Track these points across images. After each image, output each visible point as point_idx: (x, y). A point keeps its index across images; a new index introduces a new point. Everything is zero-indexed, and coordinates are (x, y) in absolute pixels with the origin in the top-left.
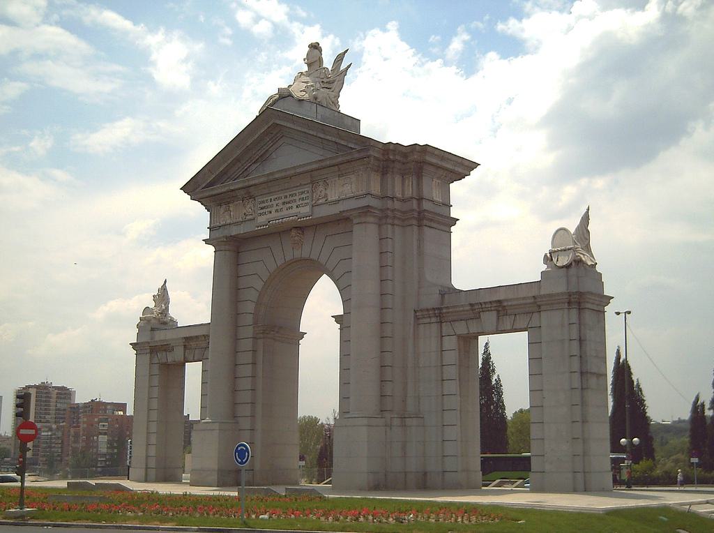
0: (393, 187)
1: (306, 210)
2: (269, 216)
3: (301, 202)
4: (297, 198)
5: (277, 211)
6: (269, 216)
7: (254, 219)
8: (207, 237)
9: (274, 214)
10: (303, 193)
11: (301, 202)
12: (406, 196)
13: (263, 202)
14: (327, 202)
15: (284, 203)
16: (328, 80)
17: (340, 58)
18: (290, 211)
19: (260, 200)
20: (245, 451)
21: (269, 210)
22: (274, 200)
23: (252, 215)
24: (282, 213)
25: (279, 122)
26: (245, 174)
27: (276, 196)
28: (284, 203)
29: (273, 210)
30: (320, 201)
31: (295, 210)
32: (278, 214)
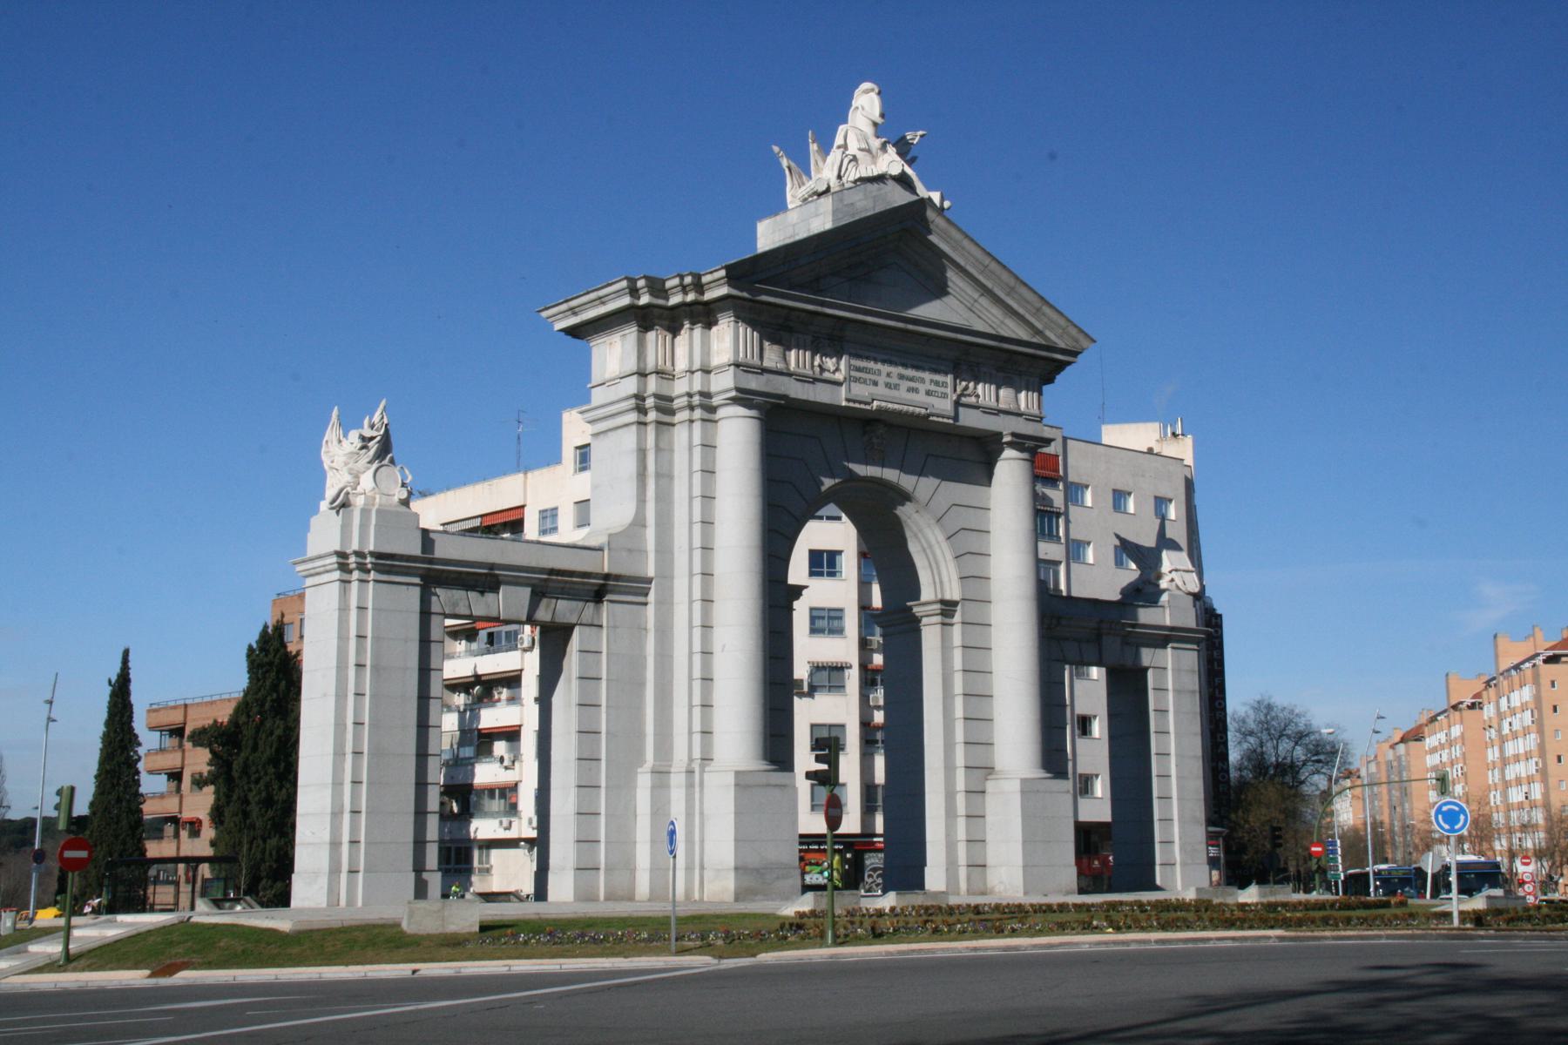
1: (946, 406)
3: (933, 388)
5: (888, 385)
6: (872, 389)
9: (881, 390)
11: (933, 388)
15: (901, 377)
20: (1442, 813)
21: (874, 377)
24: (894, 393)
28: (901, 377)
29: (882, 380)
31: (921, 398)
32: (887, 392)
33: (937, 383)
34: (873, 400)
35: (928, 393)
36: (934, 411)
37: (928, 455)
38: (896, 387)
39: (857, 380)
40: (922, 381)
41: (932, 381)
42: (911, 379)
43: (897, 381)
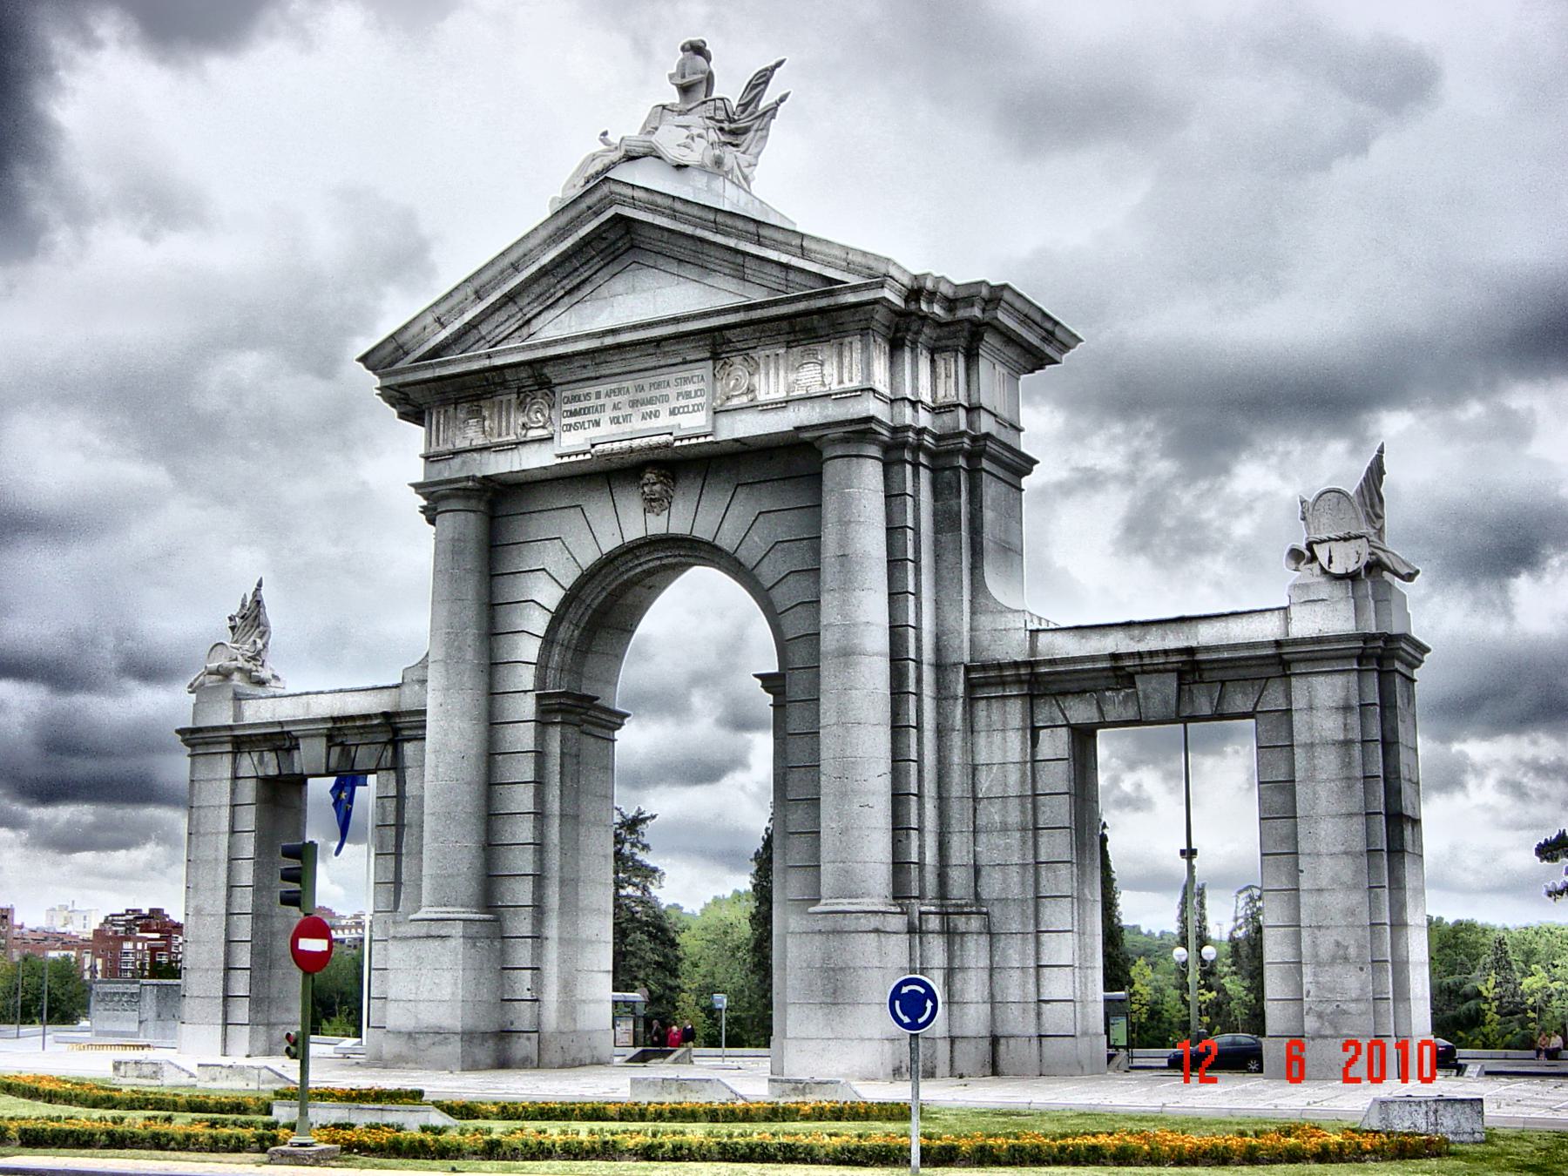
0: (915, 377)
2: (593, 433)
3: (683, 402)
4: (671, 392)
7: (551, 439)
8: (420, 479)
10: (686, 380)
12: (941, 400)
13: (576, 399)
14: (753, 407)
15: (634, 404)
16: (733, 126)
17: (761, 80)
18: (653, 423)
19: (564, 394)
22: (608, 395)
23: (543, 427)
24: (625, 428)
25: (628, 212)
26: (525, 331)
27: (614, 386)
29: (604, 418)
30: (735, 402)
31: (664, 421)
32: (615, 428)
33: (688, 395)
34: (593, 446)
35: (673, 412)
36: (681, 433)
37: (738, 485)
38: (627, 418)
39: (570, 427)
40: (666, 399)
41: (679, 394)
42: (650, 402)
43: (629, 411)
